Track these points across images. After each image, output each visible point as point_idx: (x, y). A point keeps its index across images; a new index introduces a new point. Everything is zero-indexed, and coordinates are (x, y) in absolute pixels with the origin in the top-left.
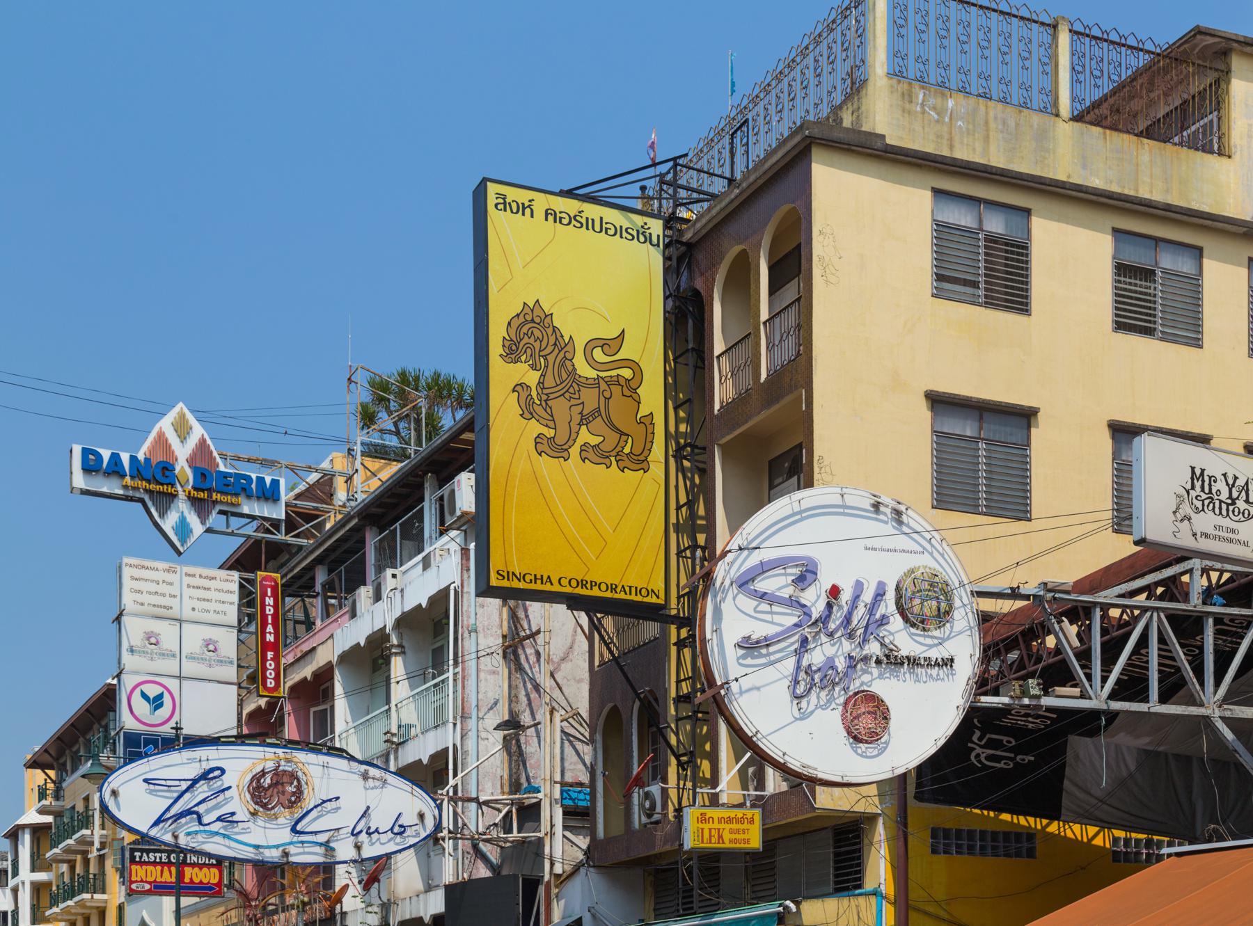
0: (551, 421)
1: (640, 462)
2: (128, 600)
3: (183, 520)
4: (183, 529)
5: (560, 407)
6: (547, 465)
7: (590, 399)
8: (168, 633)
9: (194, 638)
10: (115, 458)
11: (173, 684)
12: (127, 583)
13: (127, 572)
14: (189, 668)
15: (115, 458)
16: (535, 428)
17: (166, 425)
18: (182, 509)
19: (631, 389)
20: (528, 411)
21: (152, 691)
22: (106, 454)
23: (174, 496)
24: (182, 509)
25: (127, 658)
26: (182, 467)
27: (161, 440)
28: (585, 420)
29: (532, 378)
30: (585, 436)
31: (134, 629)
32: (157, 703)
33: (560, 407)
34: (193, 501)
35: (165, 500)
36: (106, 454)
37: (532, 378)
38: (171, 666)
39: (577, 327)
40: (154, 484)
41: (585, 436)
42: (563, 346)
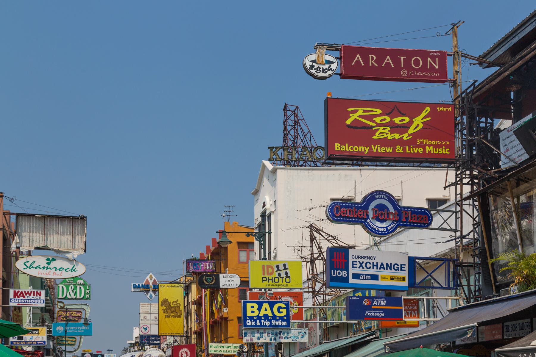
0: (167, 313)
1: (180, 316)
2: (141, 312)
3: (151, 295)
4: (151, 296)
5: (169, 311)
6: (167, 319)
7: (173, 309)
8: (148, 316)
9: (153, 316)
10: (139, 285)
11: (149, 326)
12: (141, 308)
13: (141, 305)
14: (152, 322)
15: (139, 285)
16: (165, 314)
17: (148, 277)
18: (151, 292)
19: (179, 307)
20: (164, 312)
21: (145, 327)
22: (137, 285)
23: (149, 291)
24: (151, 292)
25: (141, 322)
26: (151, 285)
27: (147, 280)
28: (172, 312)
29: (165, 308)
30: (172, 314)
31: (142, 316)
32: (146, 329)
33: (169, 311)
34: (153, 291)
35: (147, 292)
36: (137, 285)
37: (165, 308)
38: (149, 322)
39: (171, 300)
40: (146, 288)
41: (172, 314)
42: (169, 303)
